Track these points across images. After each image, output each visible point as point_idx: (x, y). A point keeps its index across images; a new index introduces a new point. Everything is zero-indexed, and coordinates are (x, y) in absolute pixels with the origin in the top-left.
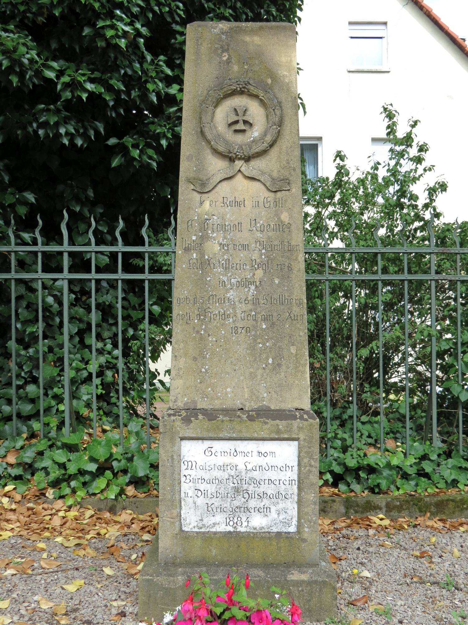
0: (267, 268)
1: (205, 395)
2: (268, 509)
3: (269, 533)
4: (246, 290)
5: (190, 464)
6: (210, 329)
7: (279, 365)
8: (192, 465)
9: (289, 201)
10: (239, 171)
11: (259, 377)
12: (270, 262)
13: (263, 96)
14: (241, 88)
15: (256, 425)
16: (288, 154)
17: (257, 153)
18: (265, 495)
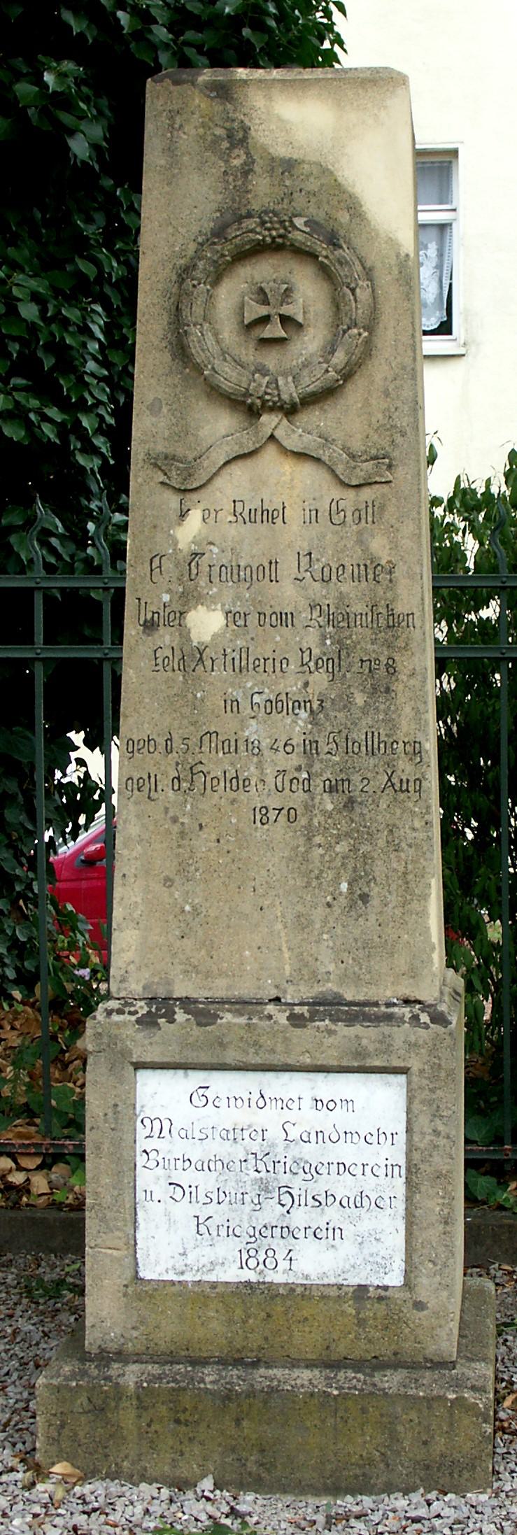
0: (336, 669)
1: (191, 969)
2: (338, 1231)
3: (340, 1287)
4: (289, 720)
5: (157, 1124)
6: (203, 812)
7: (365, 898)
8: (163, 1128)
9: (391, 509)
10: (272, 437)
11: (318, 926)
12: (344, 653)
13: (326, 257)
14: (273, 238)
15: (303, 1037)
16: (387, 394)
17: (313, 394)
18: (331, 1199)
